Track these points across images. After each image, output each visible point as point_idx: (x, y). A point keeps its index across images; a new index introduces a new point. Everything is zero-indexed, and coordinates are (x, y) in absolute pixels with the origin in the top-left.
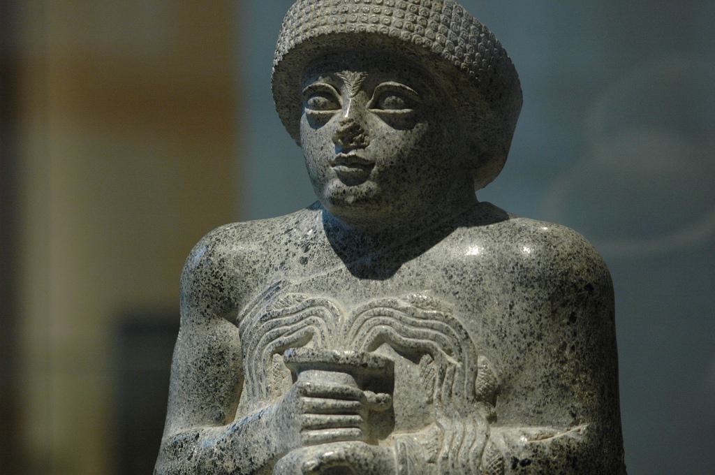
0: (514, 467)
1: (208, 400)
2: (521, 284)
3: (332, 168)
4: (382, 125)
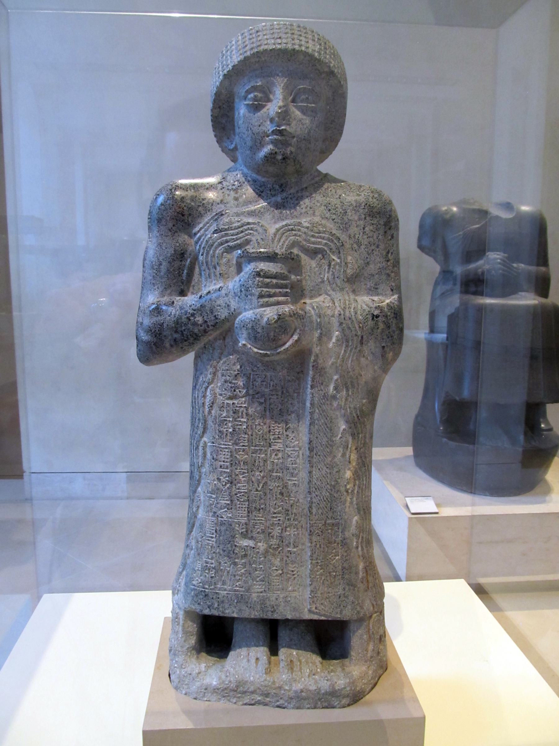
0: (373, 319)
1: (174, 281)
2: (369, 215)
3: (267, 139)
4: (298, 113)
